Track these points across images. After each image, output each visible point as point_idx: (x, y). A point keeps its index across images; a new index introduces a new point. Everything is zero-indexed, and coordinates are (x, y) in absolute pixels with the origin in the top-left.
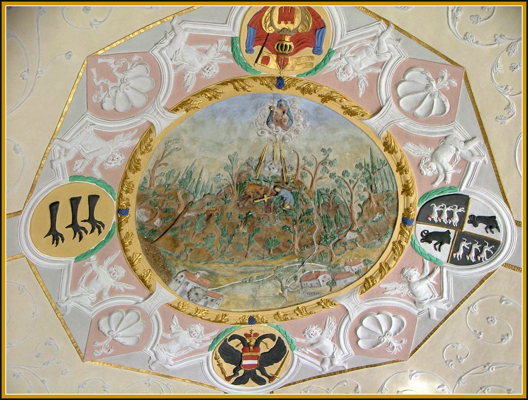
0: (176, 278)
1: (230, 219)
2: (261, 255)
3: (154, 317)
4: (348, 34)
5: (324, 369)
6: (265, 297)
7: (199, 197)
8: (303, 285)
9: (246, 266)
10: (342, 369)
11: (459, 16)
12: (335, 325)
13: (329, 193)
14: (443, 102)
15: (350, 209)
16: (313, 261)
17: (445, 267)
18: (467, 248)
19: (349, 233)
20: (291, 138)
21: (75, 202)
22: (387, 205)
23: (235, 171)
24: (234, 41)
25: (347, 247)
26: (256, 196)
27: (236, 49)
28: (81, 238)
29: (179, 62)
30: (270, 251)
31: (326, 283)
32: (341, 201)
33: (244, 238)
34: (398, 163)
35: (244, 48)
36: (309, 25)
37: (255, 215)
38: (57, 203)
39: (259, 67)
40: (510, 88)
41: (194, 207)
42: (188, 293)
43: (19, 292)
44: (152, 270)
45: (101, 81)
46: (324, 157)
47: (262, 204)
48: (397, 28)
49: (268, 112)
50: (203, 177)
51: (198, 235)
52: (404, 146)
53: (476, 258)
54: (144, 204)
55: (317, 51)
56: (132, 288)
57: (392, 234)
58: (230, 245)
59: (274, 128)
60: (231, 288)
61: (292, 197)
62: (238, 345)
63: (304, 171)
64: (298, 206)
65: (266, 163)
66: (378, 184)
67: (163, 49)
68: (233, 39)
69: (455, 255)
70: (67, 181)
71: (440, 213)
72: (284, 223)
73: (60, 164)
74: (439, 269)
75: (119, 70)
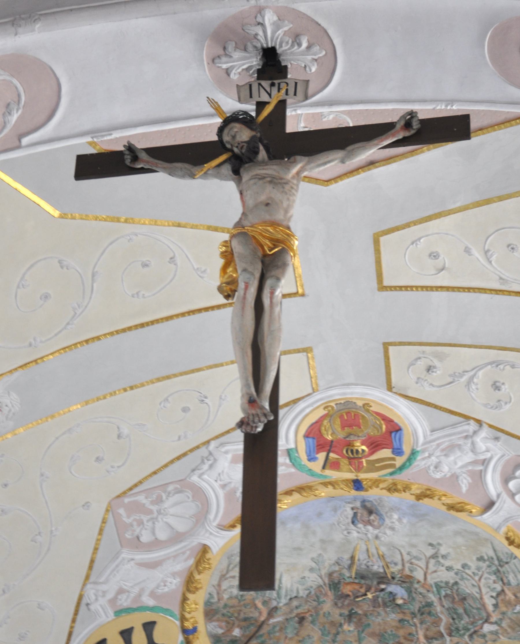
7: (284, 601)
23: (323, 572)
37: (360, 612)
39: (328, 472)
41: (279, 612)
48: (491, 426)
55: (398, 452)
64: (413, 599)
67: (203, 474)
72: (401, 616)
75: (153, 503)
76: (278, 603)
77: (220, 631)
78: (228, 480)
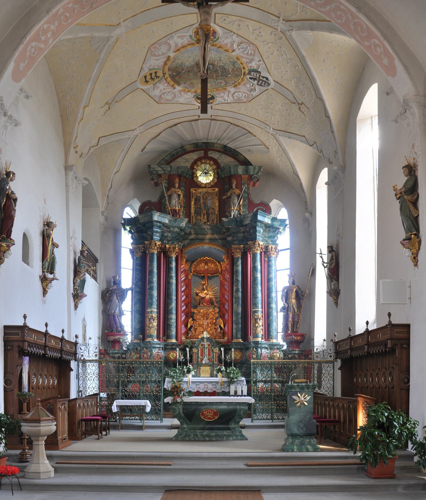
7: (185, 68)
21: (151, 74)
23: (195, 62)
28: (154, 80)
48: (237, 34)
55: (215, 37)
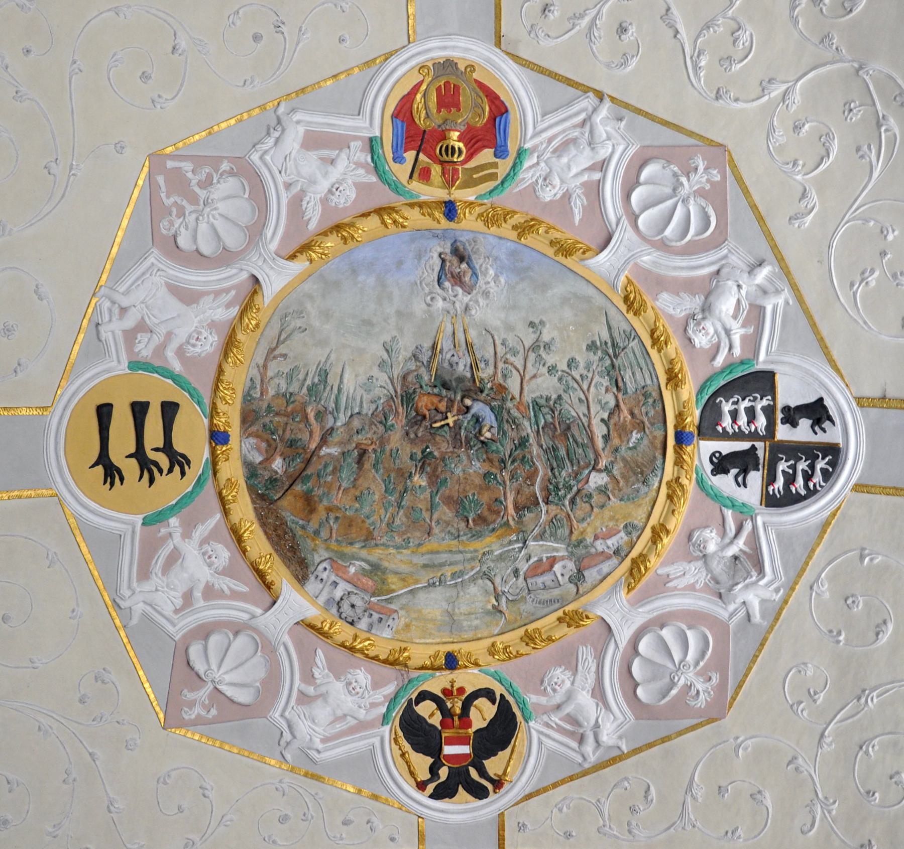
0: (316, 573)
1: (397, 461)
2: (454, 531)
3: (282, 649)
4: (543, 121)
5: (586, 755)
6: (470, 614)
7: (342, 419)
8: (530, 585)
9: (432, 552)
10: (616, 753)
11: (703, 63)
12: (593, 661)
13: (552, 403)
14: (704, 209)
15: (588, 430)
16: (541, 537)
17: (758, 514)
18: (788, 473)
19: (593, 474)
20: (479, 306)
21: (139, 410)
22: (647, 414)
23: (397, 372)
24: (374, 142)
25: (593, 501)
26: (435, 416)
27: (378, 157)
28: (152, 481)
29: (292, 176)
30: (468, 521)
31: (567, 577)
32: (573, 417)
33: (422, 497)
34: (652, 330)
35: (389, 155)
36: (484, 111)
37: (436, 454)
38: (109, 406)
39: (416, 186)
40: (801, 162)
41: (336, 438)
42: (338, 603)
43: (48, 563)
44: (275, 555)
45: (172, 200)
46: (533, 337)
47: (446, 433)
48: (613, 99)
49: (437, 263)
50: (345, 381)
51: (346, 490)
52: (658, 300)
53: (806, 486)
54: (254, 429)
55: (501, 152)
56: (244, 589)
57: (663, 469)
58: (401, 512)
59: (450, 290)
60: (410, 596)
61: (493, 418)
62: (432, 715)
63: (507, 365)
64: (504, 433)
65: (444, 354)
66: (627, 377)
67: (266, 152)
68: (371, 140)
69: (771, 489)
70: (123, 368)
71: (734, 415)
72: (486, 467)
73: (113, 330)
74: (749, 521)
75: (201, 185)
76: (335, 419)
77: (258, 458)
78: (293, 177)
